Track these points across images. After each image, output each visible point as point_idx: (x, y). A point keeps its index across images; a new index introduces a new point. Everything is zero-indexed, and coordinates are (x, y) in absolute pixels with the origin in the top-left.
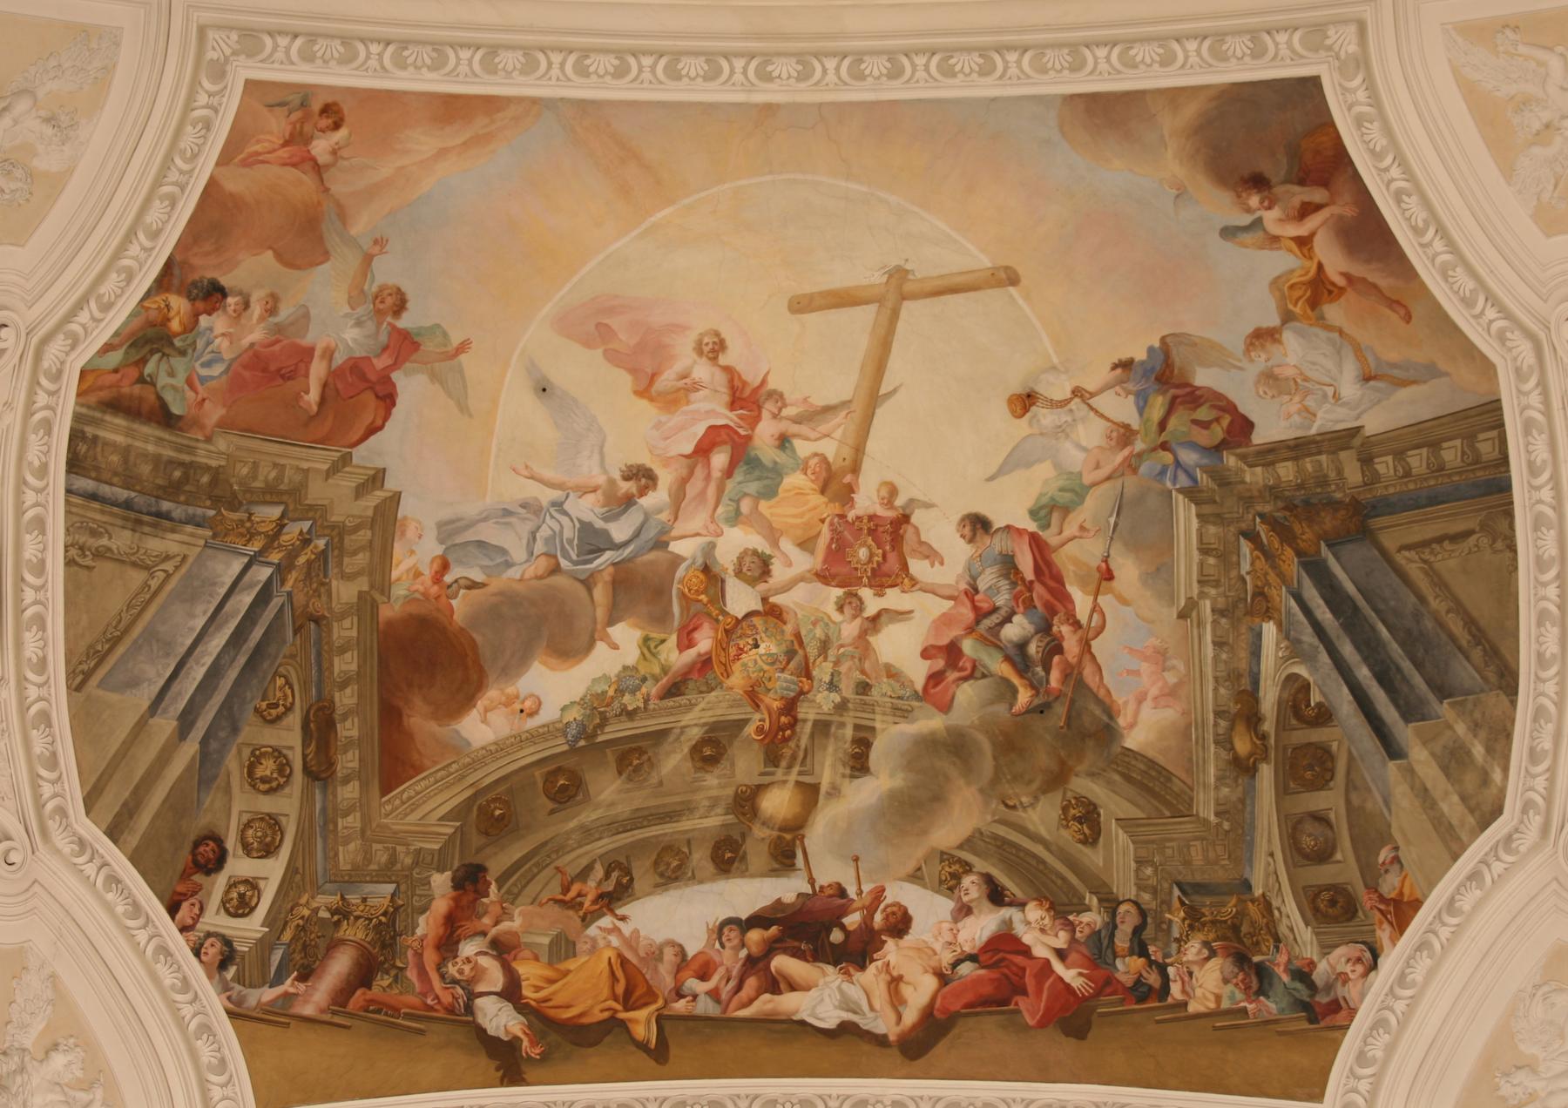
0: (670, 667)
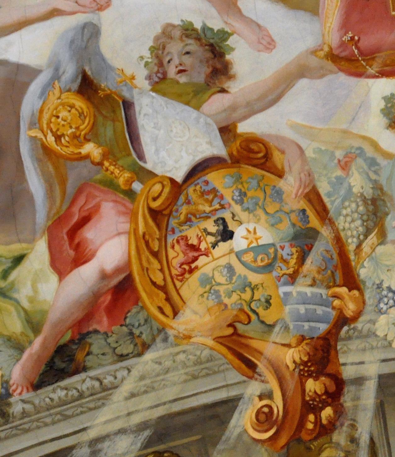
0: (44, 313)
